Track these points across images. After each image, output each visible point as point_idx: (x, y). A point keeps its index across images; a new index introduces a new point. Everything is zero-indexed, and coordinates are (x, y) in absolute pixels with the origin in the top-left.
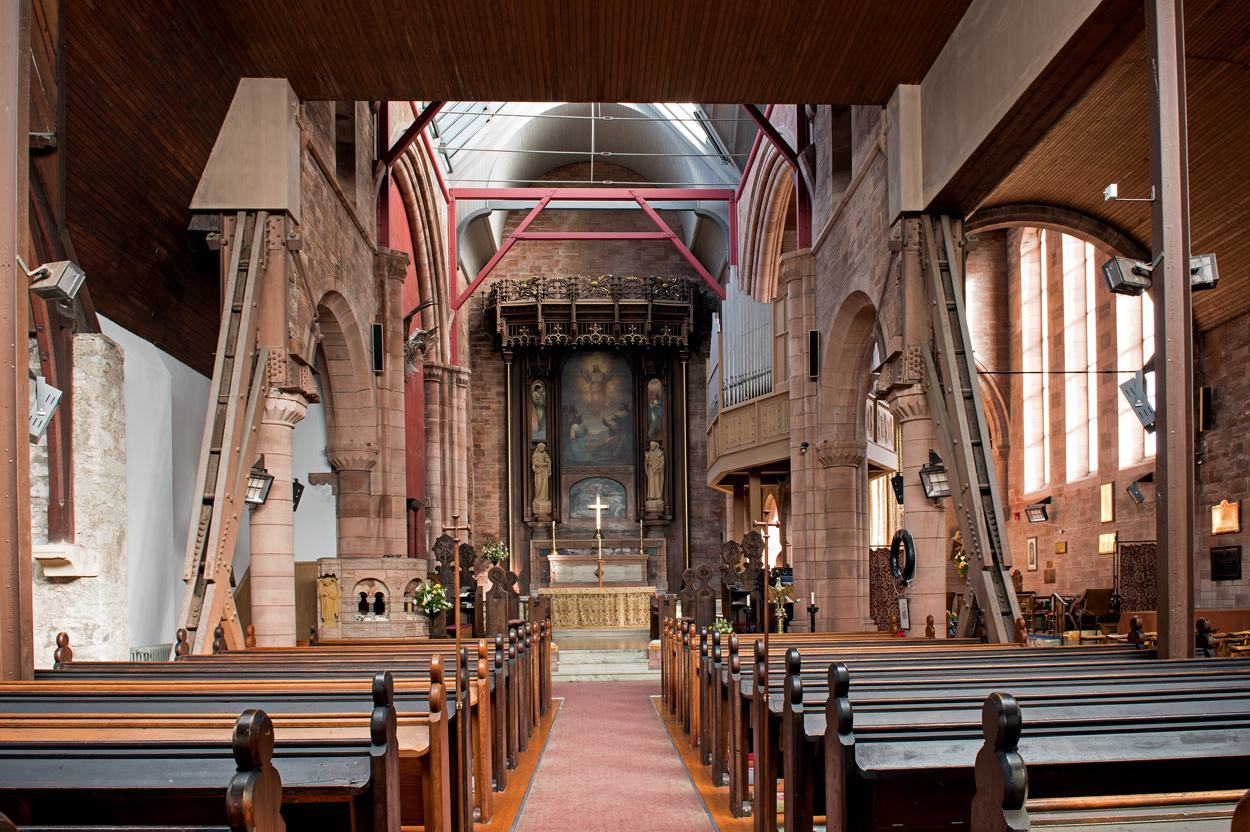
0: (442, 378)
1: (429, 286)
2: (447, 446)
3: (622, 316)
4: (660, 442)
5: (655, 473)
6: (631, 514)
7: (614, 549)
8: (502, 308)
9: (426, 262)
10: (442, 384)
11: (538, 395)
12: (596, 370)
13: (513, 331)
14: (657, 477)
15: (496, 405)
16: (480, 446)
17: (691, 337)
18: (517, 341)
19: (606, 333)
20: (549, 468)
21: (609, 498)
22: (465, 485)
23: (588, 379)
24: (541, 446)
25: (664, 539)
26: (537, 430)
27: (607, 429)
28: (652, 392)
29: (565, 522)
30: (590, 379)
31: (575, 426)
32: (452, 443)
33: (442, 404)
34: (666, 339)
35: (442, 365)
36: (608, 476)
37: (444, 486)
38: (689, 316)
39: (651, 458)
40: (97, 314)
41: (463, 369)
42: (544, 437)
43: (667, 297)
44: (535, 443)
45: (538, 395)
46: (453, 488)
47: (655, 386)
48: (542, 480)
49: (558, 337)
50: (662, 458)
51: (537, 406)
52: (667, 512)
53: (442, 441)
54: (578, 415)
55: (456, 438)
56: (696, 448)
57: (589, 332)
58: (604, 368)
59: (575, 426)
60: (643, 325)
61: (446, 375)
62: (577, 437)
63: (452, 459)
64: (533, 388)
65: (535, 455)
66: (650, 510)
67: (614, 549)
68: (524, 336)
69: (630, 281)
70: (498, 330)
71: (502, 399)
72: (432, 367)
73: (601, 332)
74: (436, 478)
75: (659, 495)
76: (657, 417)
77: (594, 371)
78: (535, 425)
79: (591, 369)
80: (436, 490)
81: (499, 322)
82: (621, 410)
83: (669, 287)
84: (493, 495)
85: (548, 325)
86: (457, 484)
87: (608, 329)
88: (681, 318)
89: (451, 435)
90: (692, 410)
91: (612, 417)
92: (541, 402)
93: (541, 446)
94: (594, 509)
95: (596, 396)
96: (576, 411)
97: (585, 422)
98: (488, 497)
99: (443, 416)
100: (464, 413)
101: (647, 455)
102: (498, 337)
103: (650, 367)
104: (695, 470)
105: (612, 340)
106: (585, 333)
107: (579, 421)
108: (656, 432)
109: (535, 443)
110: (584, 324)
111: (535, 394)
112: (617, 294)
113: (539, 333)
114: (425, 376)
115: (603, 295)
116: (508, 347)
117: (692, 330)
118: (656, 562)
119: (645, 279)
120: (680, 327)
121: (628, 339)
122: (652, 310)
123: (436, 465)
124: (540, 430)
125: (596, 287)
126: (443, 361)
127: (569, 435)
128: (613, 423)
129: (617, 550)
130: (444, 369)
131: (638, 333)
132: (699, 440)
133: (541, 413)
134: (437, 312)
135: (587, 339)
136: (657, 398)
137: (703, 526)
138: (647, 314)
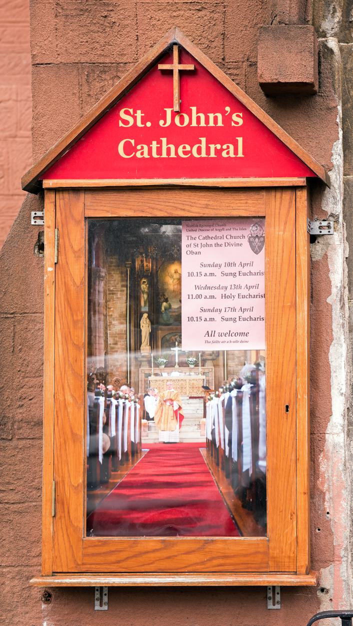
23: (172, 277)
24: (145, 315)
30: (173, 277)
31: (165, 304)
40: (101, 463)
42: (147, 310)
51: (143, 292)
54: (166, 298)
59: (165, 304)
62: (165, 309)
64: (142, 282)
71: (125, 289)
77: (175, 272)
78: (143, 304)
79: (173, 272)
92: (146, 290)
93: (145, 315)
97: (169, 302)
107: (166, 300)
127: (161, 309)
137: (234, 359)
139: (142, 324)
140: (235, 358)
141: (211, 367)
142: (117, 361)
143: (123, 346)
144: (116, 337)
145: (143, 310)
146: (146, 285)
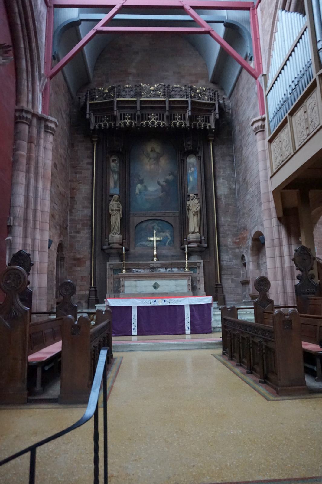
0: (31, 122)
1: (22, 46)
2: (32, 175)
3: (171, 108)
4: (196, 195)
5: (194, 215)
6: (177, 244)
7: (166, 269)
8: (90, 104)
9: (19, 22)
10: (30, 126)
11: (114, 165)
12: (153, 150)
13: (97, 119)
14: (195, 218)
15: (87, 174)
16: (74, 197)
17: (217, 122)
18: (100, 126)
19: (160, 120)
20: (121, 212)
21: (161, 233)
22: (47, 209)
23: (148, 156)
25: (202, 261)
26: (114, 188)
27: (161, 187)
28: (190, 163)
29: (132, 251)
32: (37, 174)
33: (30, 142)
34: (200, 125)
35: (32, 111)
36: (162, 218)
37: (27, 208)
38: (215, 110)
39: (191, 205)
41: (50, 118)
42: (118, 192)
43: (200, 98)
44: (112, 196)
45: (114, 165)
46: (35, 210)
47: (192, 160)
48: (116, 219)
49: (128, 122)
50: (199, 204)
51: (113, 171)
52: (203, 242)
53: (28, 172)
54: (140, 179)
55: (41, 170)
56: (221, 199)
57: (149, 119)
58: (158, 149)
60: (184, 115)
61: (35, 121)
62: (140, 193)
63: (36, 188)
65: (111, 203)
66: (191, 240)
67: (166, 269)
68: (105, 123)
69: (176, 87)
70: (88, 116)
71: (90, 167)
72: (22, 110)
73: (157, 119)
74: (20, 200)
75: (197, 230)
76: (194, 179)
77: (152, 151)
78: (112, 184)
80: (19, 211)
81: (88, 112)
82: (170, 175)
83: (200, 93)
84: (82, 231)
85: (121, 115)
86: (39, 208)
87: (161, 117)
88: (210, 111)
89: (37, 168)
90: (217, 174)
91: (163, 180)
92: (116, 170)
94: (152, 241)
95: (152, 166)
96: (140, 176)
97: (145, 184)
98: (78, 232)
99: (29, 151)
100: (50, 154)
101: (188, 203)
102: (88, 122)
103: (189, 145)
104: (221, 214)
105: (164, 124)
106: (146, 120)
107: (141, 182)
108: (193, 189)
109: (112, 196)
110: (145, 114)
111: (112, 164)
112: (167, 94)
113: (114, 118)
114: (16, 118)
115: (158, 96)
116: (94, 129)
117: (217, 116)
118: (196, 278)
119: (186, 86)
120: (209, 117)
121: (175, 124)
122: (191, 104)
123: (20, 191)
124: (115, 187)
125: (153, 91)
126: (33, 107)
127: (135, 192)
128: (164, 184)
129: (168, 269)
130: (34, 115)
131: (181, 120)
132: (223, 193)
133: (116, 176)
134: (30, 69)
135: (147, 124)
136: (194, 167)
137: (228, 252)
138: (188, 107)
139: (111, 207)
140: (229, 250)
141: (199, 261)
142: (79, 253)
143: (87, 235)
144: (79, 224)
145: (112, 192)
146: (116, 164)
